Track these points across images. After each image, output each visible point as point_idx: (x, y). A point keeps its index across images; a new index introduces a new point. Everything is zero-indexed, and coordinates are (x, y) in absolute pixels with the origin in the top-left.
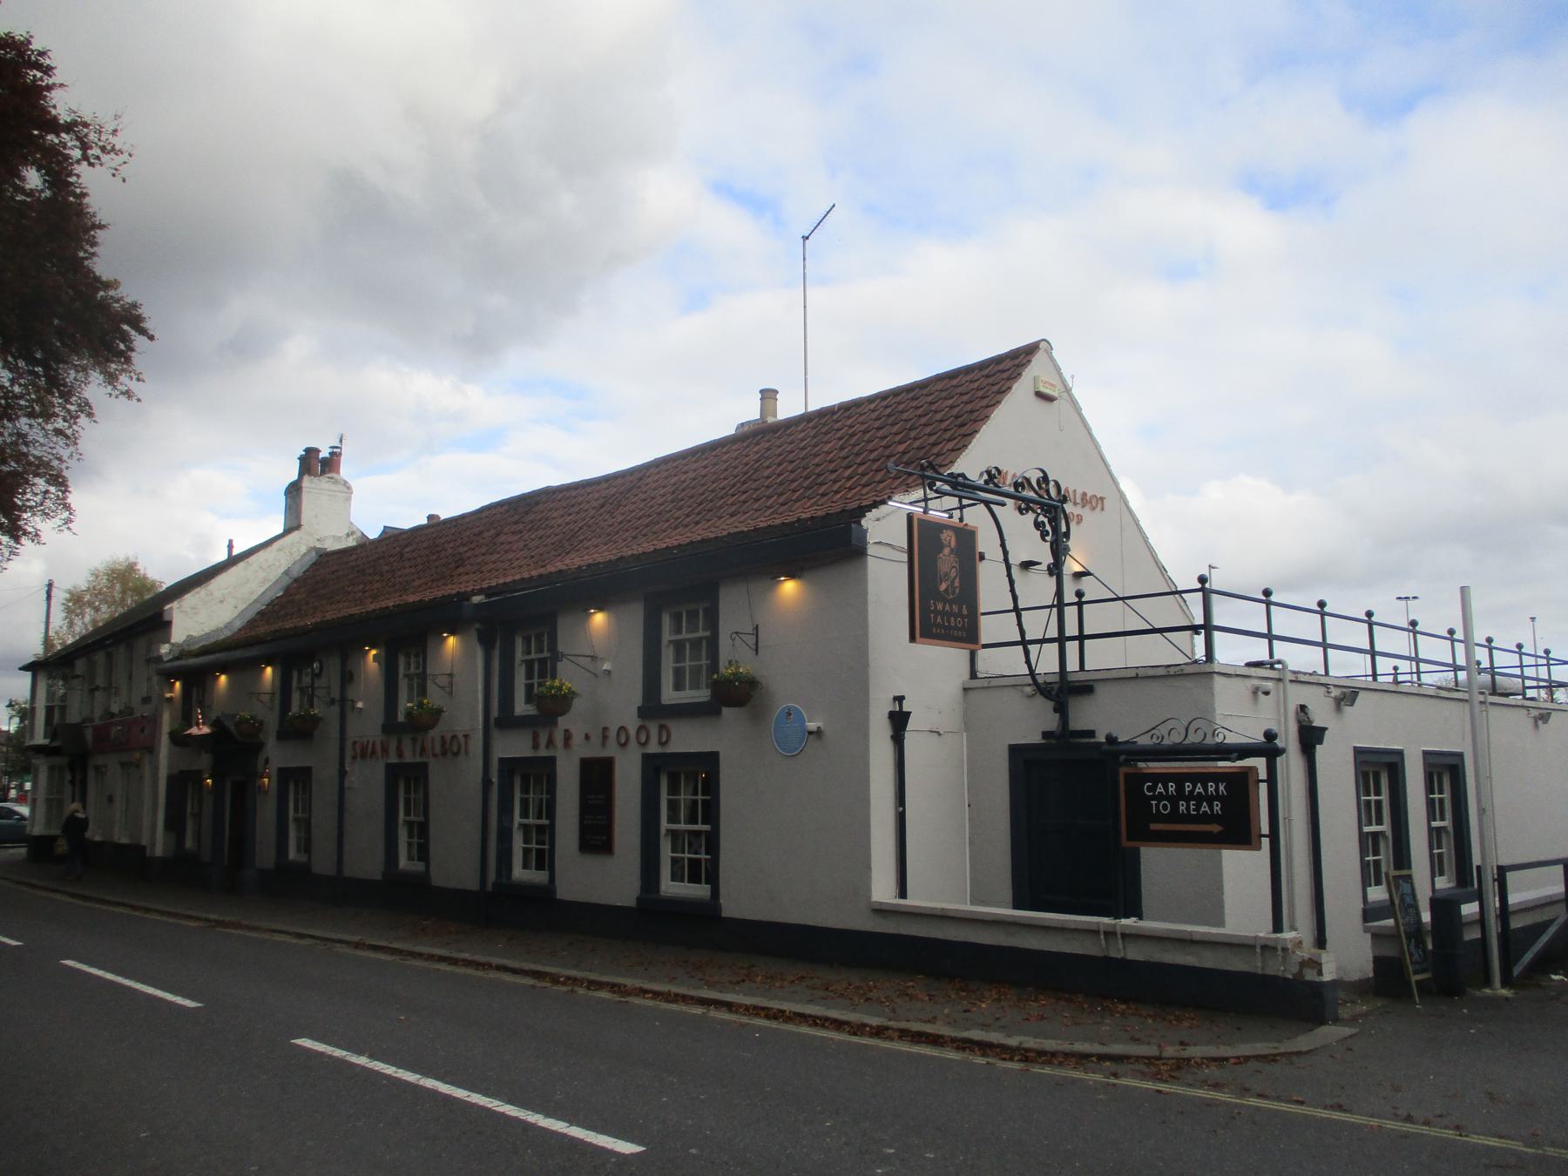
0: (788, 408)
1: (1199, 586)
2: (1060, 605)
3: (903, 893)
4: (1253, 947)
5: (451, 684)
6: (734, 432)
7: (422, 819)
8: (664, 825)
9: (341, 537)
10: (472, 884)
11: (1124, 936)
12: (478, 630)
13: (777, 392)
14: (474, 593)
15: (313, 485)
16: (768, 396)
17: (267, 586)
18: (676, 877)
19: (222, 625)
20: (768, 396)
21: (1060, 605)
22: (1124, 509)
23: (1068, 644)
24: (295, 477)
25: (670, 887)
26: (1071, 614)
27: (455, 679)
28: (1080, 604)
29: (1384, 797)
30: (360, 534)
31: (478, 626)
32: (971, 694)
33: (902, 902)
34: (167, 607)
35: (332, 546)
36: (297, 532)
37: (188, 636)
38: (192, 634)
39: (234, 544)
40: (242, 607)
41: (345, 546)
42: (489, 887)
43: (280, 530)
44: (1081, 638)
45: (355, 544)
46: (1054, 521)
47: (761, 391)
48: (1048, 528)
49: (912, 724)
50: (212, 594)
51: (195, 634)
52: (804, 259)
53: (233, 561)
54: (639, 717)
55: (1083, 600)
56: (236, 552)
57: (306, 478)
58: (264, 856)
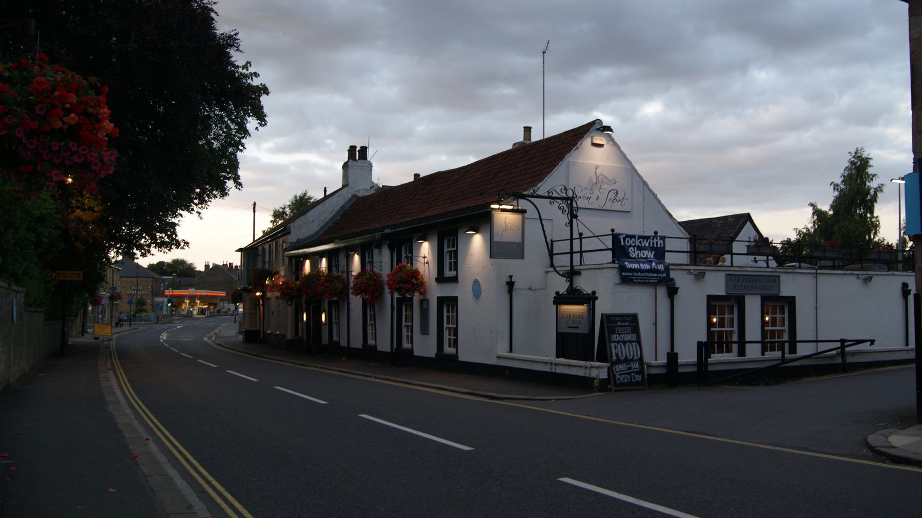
0: (536, 137)
1: (611, 233)
2: (572, 239)
3: (511, 351)
4: (583, 367)
5: (381, 266)
6: (511, 148)
7: (455, 326)
8: (445, 325)
9: (367, 189)
10: (389, 350)
11: (556, 364)
12: (388, 244)
13: (531, 128)
14: (387, 227)
15: (353, 164)
16: (528, 130)
17: (334, 213)
18: (450, 346)
19: (313, 233)
20: (528, 130)
21: (572, 239)
22: (645, 188)
23: (574, 255)
24: (347, 160)
25: (448, 350)
26: (576, 243)
27: (383, 264)
28: (581, 239)
29: (455, 314)
30: (376, 187)
31: (388, 242)
32: (549, 273)
33: (510, 354)
34: (288, 226)
35: (360, 195)
36: (346, 188)
37: (298, 239)
38: (299, 237)
39: (327, 189)
40: (322, 224)
41: (370, 194)
42: (394, 351)
43: (341, 186)
44: (581, 252)
45: (374, 192)
46: (571, 204)
47: (524, 128)
48: (566, 208)
49: (516, 286)
50: (308, 219)
51: (301, 238)
52: (544, 63)
53: (326, 197)
54: (436, 281)
55: (583, 236)
56: (328, 193)
57: (350, 161)
58: (325, 340)
